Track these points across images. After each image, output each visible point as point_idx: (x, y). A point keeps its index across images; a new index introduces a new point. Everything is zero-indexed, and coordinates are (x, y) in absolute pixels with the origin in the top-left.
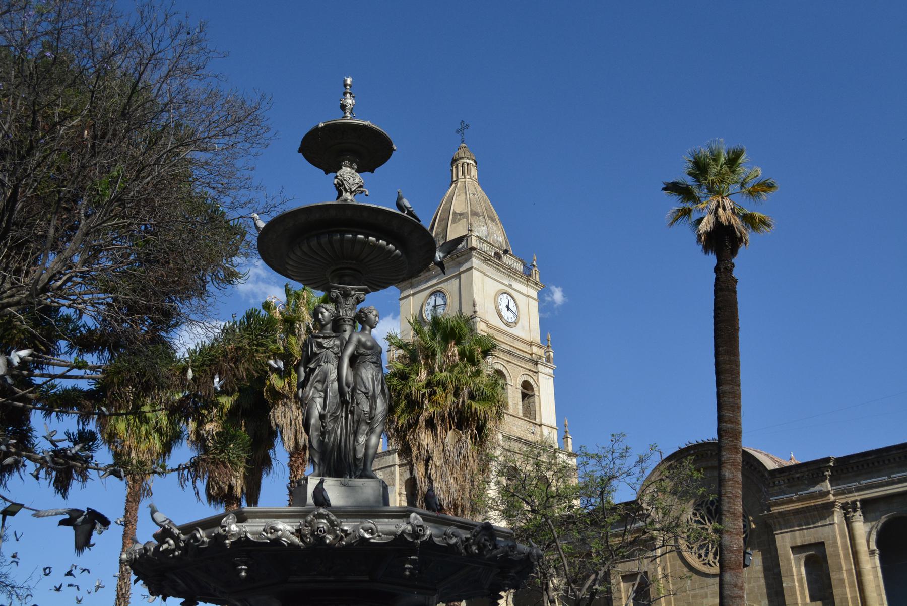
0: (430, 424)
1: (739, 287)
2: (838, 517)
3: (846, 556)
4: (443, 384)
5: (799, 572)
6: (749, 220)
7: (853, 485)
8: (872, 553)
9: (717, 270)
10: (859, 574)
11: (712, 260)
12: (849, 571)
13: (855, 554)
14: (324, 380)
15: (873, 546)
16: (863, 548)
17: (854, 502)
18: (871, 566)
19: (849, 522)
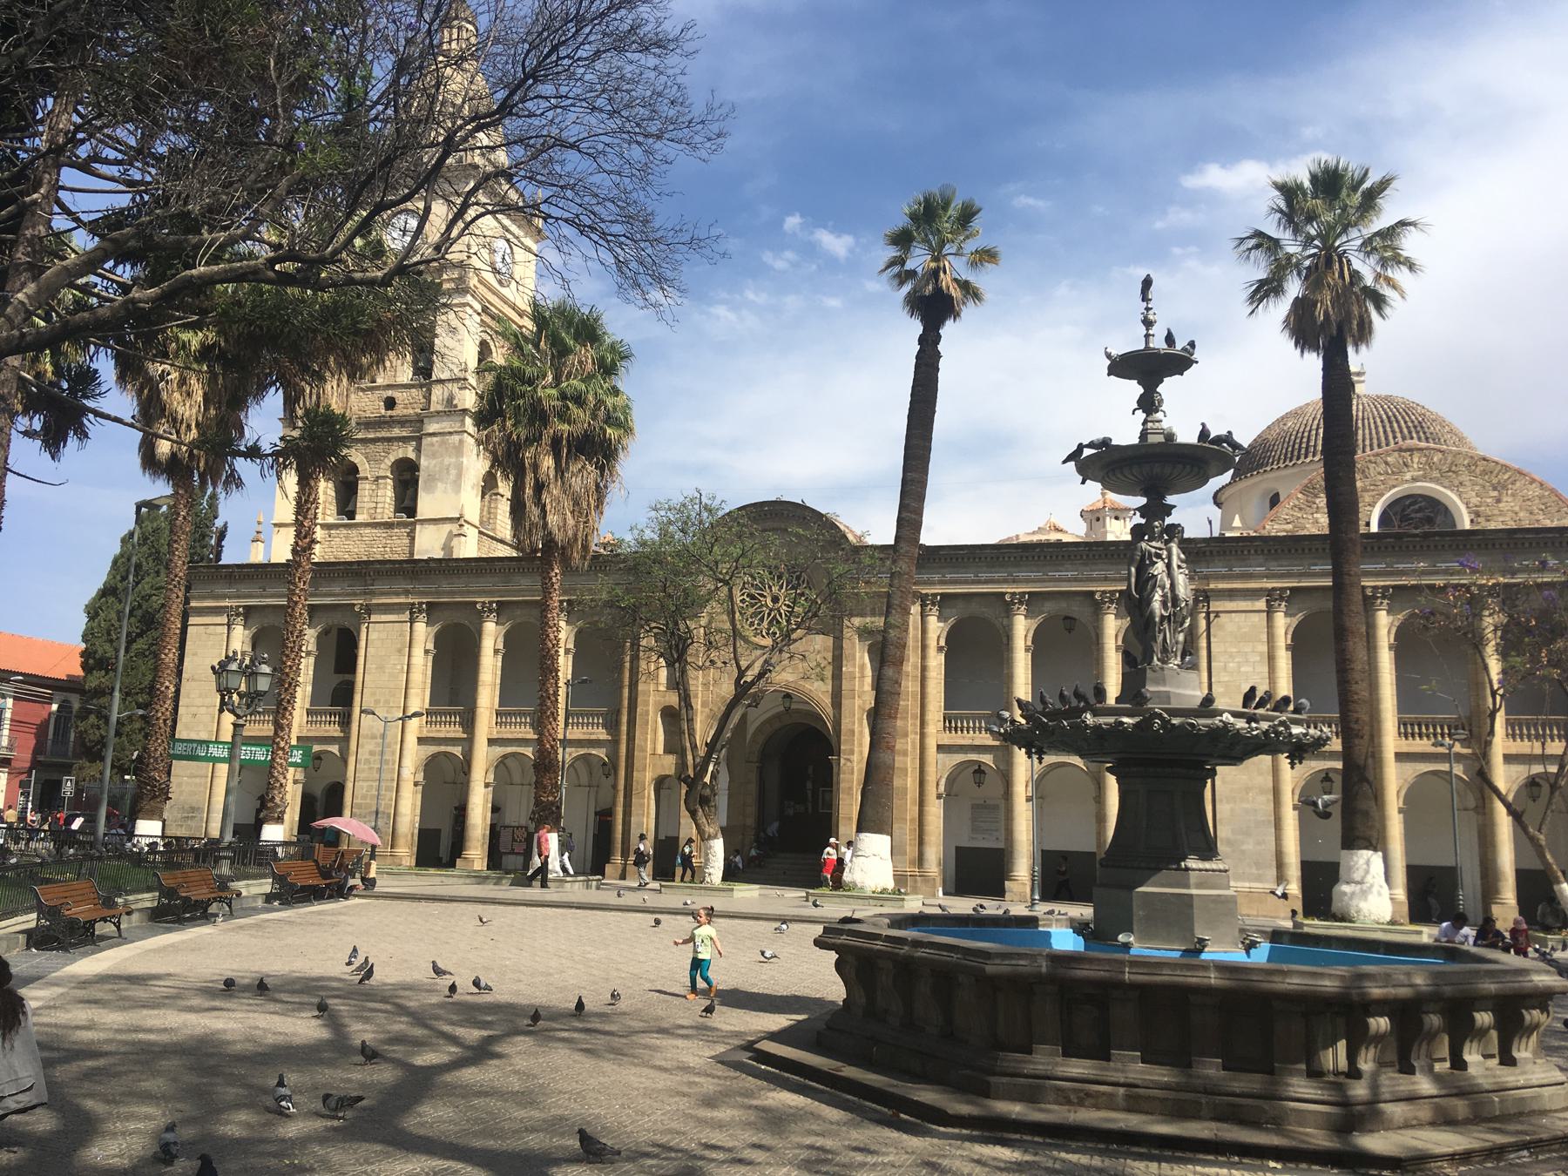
0: (556, 444)
1: (942, 364)
2: (915, 609)
3: (915, 648)
4: (579, 400)
5: (862, 657)
6: (965, 286)
7: (937, 577)
8: (940, 649)
9: (921, 340)
10: (924, 669)
11: (916, 327)
12: (915, 667)
13: (924, 647)
14: (1163, 588)
15: (942, 643)
16: (932, 644)
17: (935, 595)
18: (936, 662)
19: (923, 616)
